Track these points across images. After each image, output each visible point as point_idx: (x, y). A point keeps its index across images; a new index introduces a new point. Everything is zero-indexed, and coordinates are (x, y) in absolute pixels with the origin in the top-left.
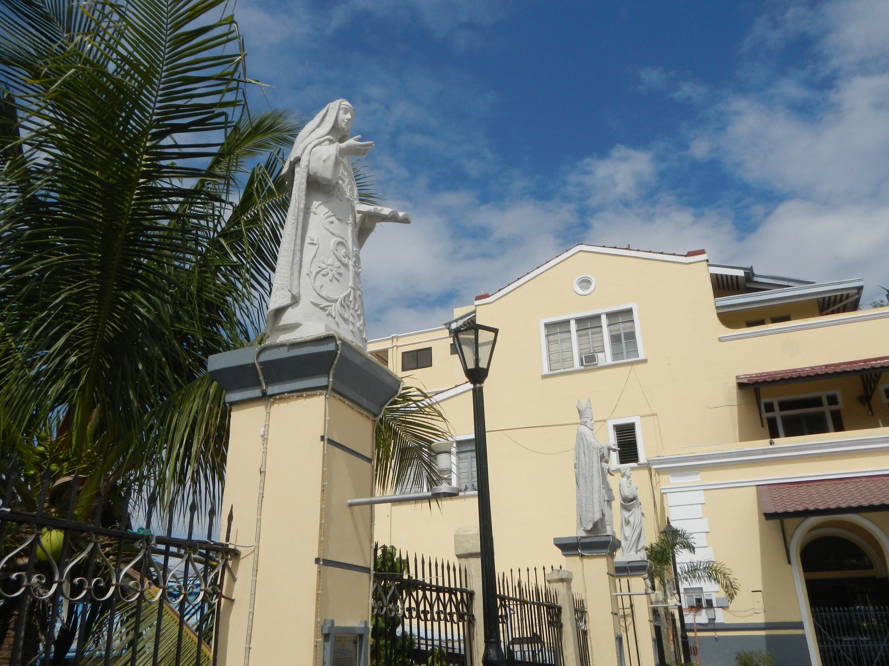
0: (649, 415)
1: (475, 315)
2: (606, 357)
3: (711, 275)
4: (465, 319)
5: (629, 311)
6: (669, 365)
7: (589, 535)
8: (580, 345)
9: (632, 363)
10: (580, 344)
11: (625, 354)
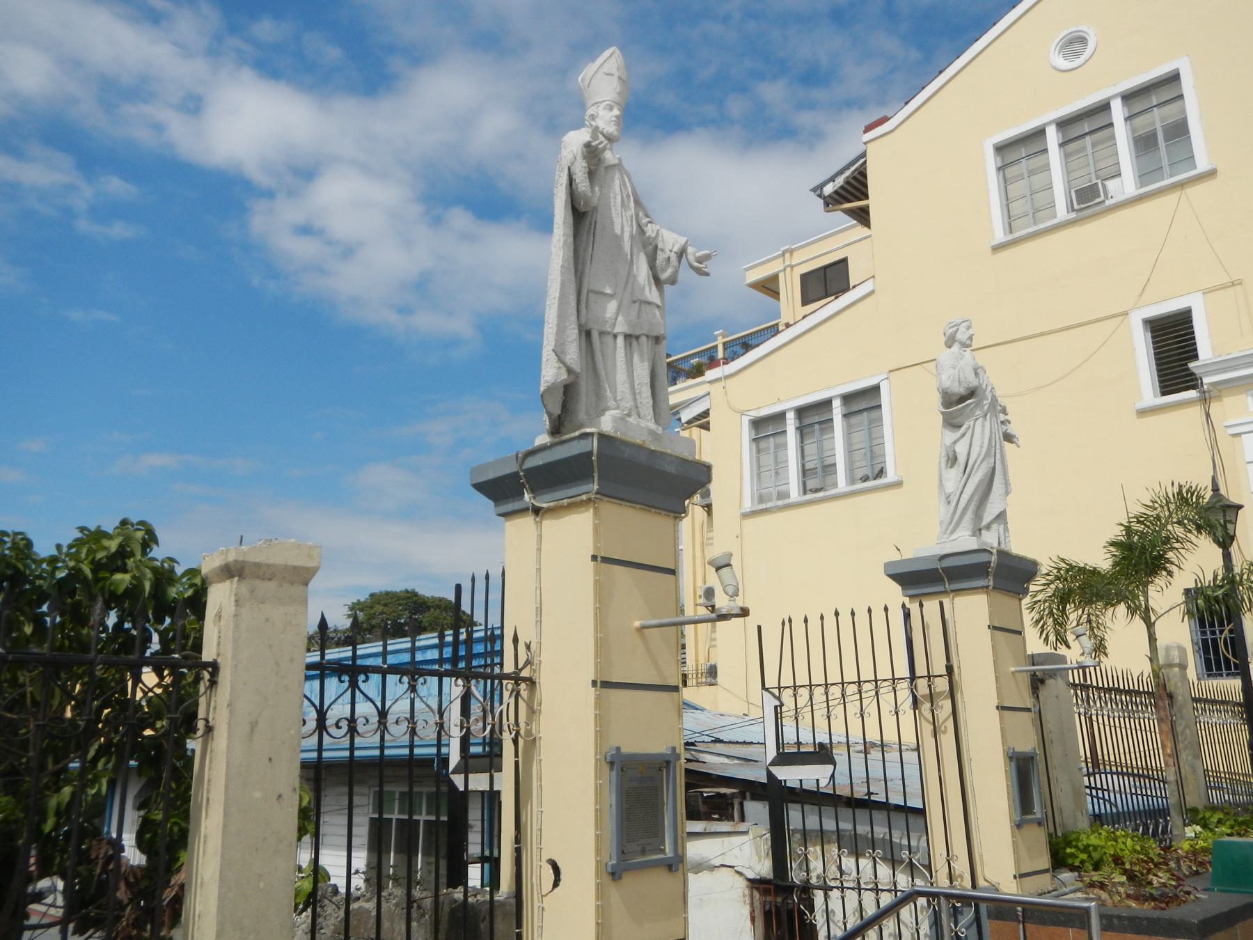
0: (1224, 287)
1: (866, 161)
2: (1125, 185)
4: (848, 173)
5: (1173, 78)
7: (557, 440)
8: (1068, 173)
9: (1181, 185)
10: (1068, 171)
11: (1166, 169)
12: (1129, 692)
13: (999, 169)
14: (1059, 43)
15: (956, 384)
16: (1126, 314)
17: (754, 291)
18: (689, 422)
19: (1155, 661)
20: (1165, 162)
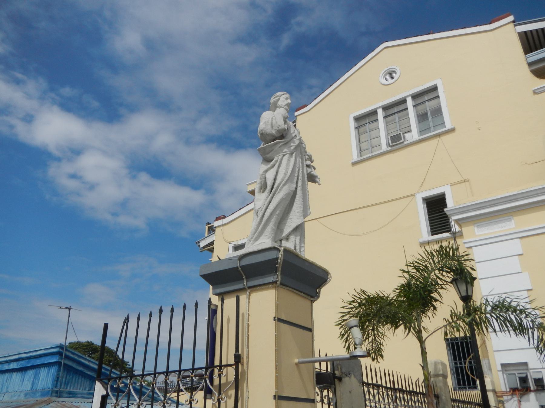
0: (460, 183)
2: (414, 135)
3: (520, 34)
5: (435, 89)
6: (479, 129)
8: (387, 130)
9: (439, 135)
12: (410, 393)
13: (356, 128)
14: (383, 73)
15: (269, 127)
16: (414, 195)
17: (249, 194)
18: (204, 247)
19: (425, 368)
20: (431, 126)
